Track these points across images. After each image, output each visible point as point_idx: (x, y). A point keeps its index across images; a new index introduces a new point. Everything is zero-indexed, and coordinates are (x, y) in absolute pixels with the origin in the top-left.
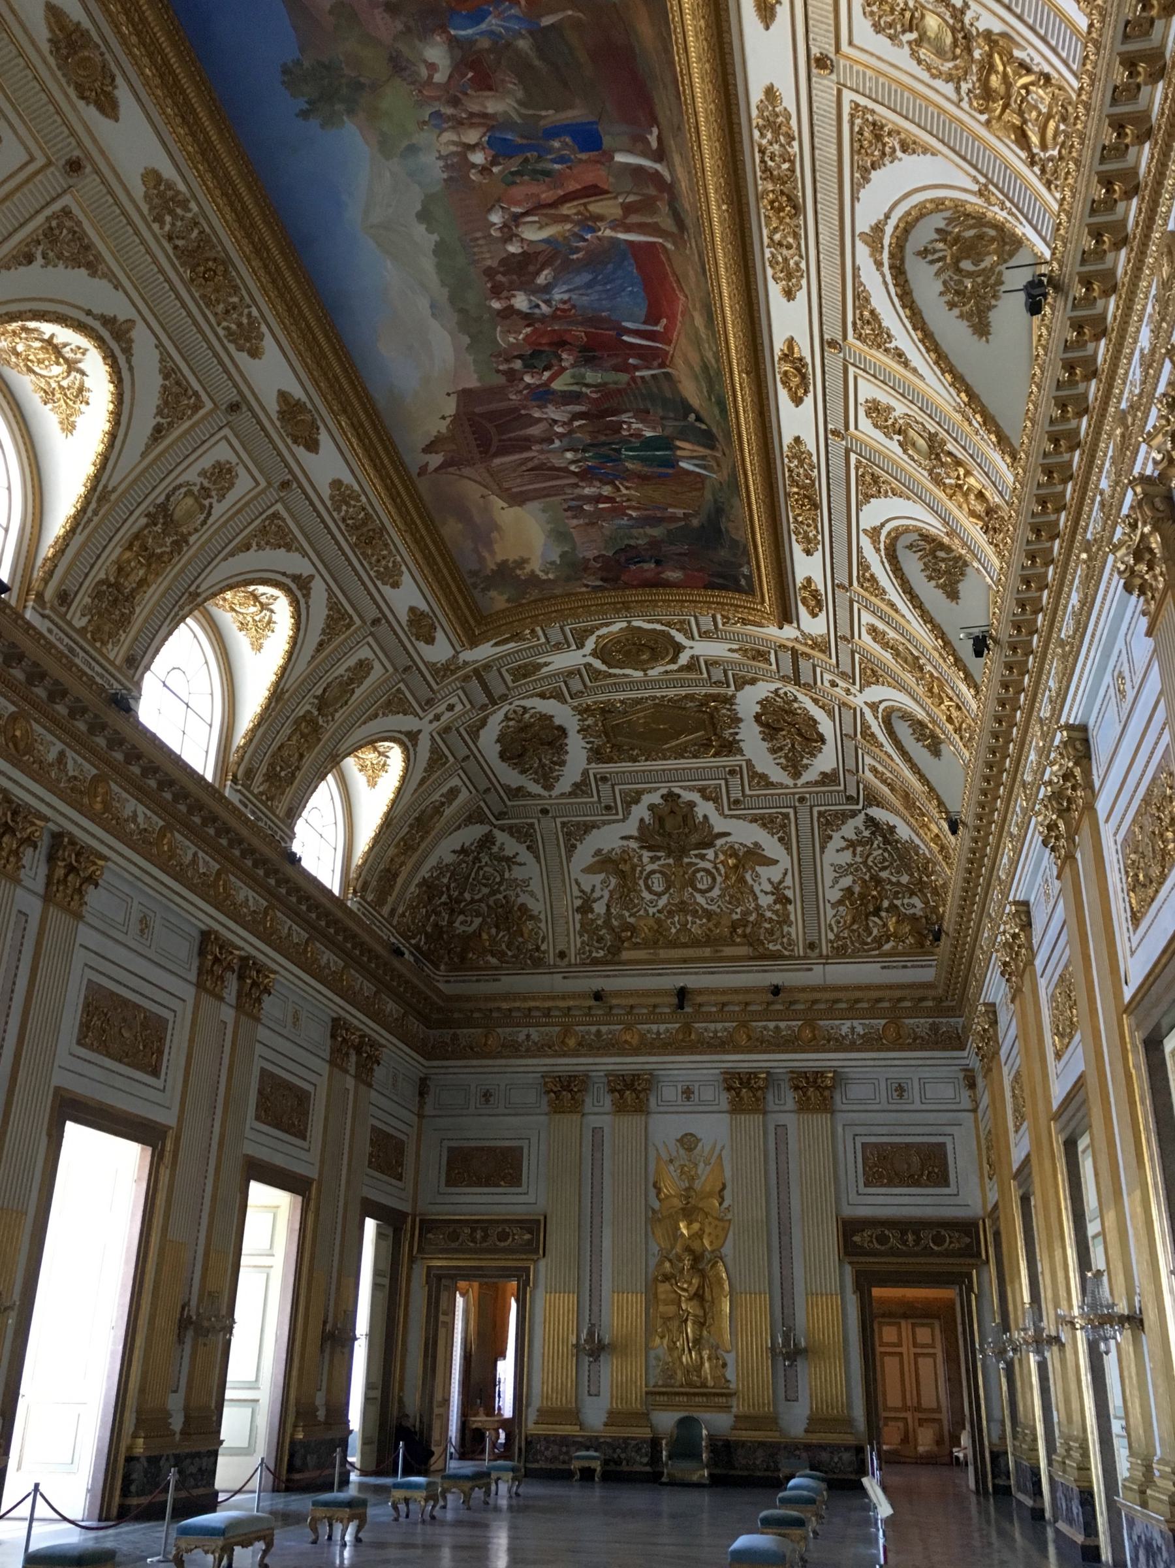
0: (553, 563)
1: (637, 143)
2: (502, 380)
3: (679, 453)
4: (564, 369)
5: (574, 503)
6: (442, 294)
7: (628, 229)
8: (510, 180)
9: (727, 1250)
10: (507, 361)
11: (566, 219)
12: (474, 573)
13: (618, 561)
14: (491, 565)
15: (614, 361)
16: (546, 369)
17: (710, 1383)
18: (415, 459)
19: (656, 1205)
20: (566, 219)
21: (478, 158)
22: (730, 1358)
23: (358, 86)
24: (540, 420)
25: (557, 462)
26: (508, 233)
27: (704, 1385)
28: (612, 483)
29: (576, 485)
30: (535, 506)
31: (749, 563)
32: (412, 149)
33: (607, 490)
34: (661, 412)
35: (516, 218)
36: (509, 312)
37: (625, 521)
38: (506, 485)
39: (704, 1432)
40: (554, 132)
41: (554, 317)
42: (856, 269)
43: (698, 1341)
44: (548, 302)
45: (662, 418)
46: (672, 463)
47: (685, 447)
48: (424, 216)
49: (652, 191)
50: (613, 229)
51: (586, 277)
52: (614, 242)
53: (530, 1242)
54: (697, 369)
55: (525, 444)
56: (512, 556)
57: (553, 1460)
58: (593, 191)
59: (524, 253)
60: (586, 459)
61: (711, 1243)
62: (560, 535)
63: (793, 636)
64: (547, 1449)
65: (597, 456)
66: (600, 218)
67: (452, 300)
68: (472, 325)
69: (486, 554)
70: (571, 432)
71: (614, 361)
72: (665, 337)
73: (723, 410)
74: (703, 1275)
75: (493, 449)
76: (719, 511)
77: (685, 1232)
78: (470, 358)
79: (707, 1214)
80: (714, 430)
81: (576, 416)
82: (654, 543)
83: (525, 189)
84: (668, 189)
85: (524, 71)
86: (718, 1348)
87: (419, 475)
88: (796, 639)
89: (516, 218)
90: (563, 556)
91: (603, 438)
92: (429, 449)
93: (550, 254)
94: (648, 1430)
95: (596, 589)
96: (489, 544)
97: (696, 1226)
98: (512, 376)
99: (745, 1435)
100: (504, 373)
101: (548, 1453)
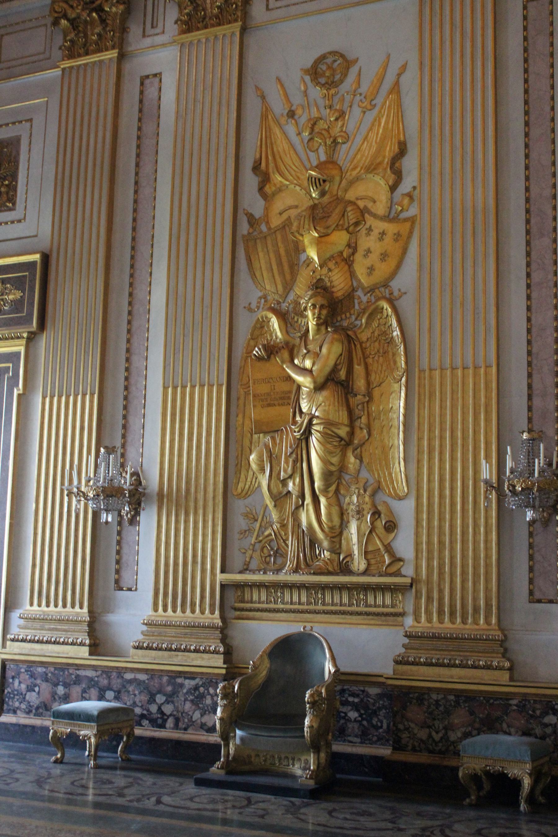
9: (406, 279)
17: (359, 563)
19: (257, 207)
22: (405, 511)
27: (345, 569)
39: (329, 667)
43: (335, 477)
53: (17, 305)
57: (43, 709)
61: (371, 269)
64: (30, 689)
74: (349, 339)
77: (313, 254)
79: (363, 212)
86: (378, 489)
94: (219, 661)
97: (340, 239)
99: (425, 676)
101: (32, 697)
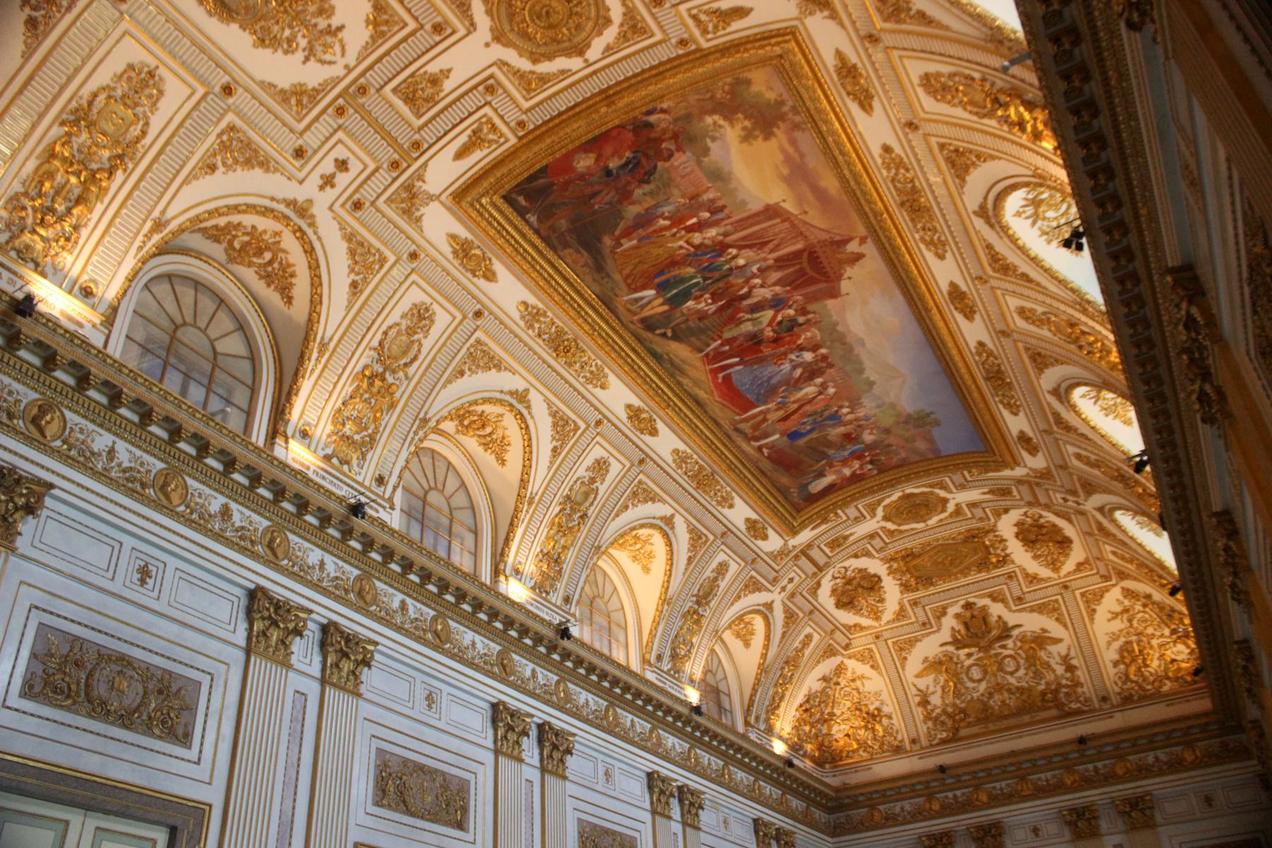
0: (714, 139)
1: (770, 446)
2: (810, 307)
3: (660, 300)
4: (770, 324)
5: (720, 216)
6: (858, 350)
7: (761, 412)
8: (827, 407)
10: (808, 321)
11: (794, 402)
12: (796, 127)
13: (647, 156)
14: (780, 133)
15: (738, 342)
16: (780, 323)
18: (869, 249)
20: (794, 402)
21: (845, 410)
23: (906, 422)
24: (775, 284)
25: (748, 253)
26: (824, 386)
28: (697, 247)
29: (726, 235)
30: (755, 206)
31: (537, 232)
32: (878, 407)
33: (697, 238)
34: (691, 323)
35: (820, 393)
36: (814, 348)
37: (666, 210)
38: (787, 225)
40: (810, 431)
41: (785, 354)
42: (664, 502)
44: (792, 361)
45: (687, 320)
46: (662, 288)
47: (658, 307)
48: (871, 384)
49: (757, 433)
50: (768, 410)
51: (773, 381)
52: (765, 403)
54: (687, 367)
55: (781, 263)
56: (759, 144)
58: (784, 419)
59: (812, 379)
60: (727, 262)
62: (719, 176)
63: (428, 177)
65: (718, 268)
66: (777, 410)
67: (851, 350)
68: (838, 337)
69: (791, 150)
70: (747, 281)
71: (738, 342)
72: (715, 372)
73: (655, 355)
75: (805, 256)
76: (599, 268)
78: (835, 318)
80: (650, 335)
81: (747, 296)
82: (626, 196)
83: (818, 406)
84: (749, 439)
85: (830, 444)
87: (866, 238)
88: (421, 178)
89: (820, 393)
90: (706, 151)
91: (721, 284)
92: (858, 257)
93: (796, 384)
95: (649, 113)
96: (788, 159)
98: (803, 311)
100: (809, 313)
